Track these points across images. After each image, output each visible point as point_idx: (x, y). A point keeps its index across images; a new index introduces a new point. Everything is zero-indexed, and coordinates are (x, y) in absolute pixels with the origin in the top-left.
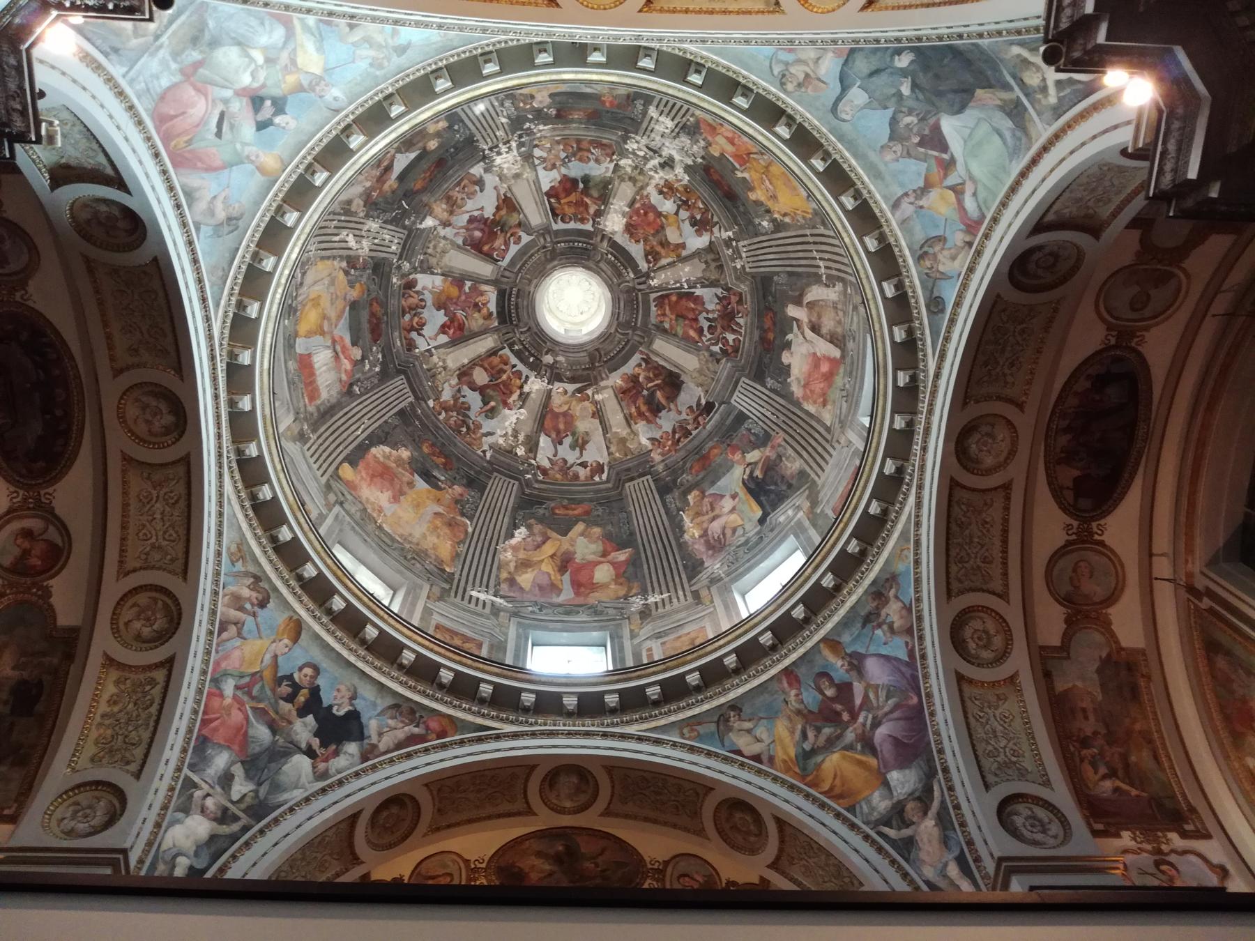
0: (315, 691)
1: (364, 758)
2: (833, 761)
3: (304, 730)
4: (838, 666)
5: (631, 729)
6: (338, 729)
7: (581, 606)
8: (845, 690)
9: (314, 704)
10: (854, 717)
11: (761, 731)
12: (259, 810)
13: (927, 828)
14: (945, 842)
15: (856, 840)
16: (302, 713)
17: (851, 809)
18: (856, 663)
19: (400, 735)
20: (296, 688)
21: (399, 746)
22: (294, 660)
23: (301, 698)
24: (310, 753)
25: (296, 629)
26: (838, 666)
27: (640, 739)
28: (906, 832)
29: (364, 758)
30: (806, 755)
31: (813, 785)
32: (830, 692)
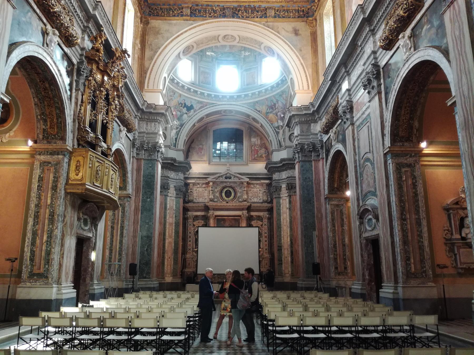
0: (185, 104)
1: (194, 112)
2: (271, 115)
3: (185, 110)
4: (275, 101)
5: (238, 103)
6: (189, 108)
7: (230, 53)
8: (275, 105)
9: (185, 106)
10: (275, 109)
11: (261, 107)
12: (182, 125)
13: (281, 131)
14: (283, 135)
15: (271, 130)
16: (184, 108)
17: (272, 124)
18: (277, 101)
19: (199, 107)
20: (182, 104)
21: (200, 109)
22: (181, 100)
23: (183, 106)
24: (186, 114)
25: (180, 95)
26: (275, 101)
27: (240, 106)
28: (279, 131)
29: (194, 112)
30: (268, 113)
31: (267, 118)
32: (273, 104)
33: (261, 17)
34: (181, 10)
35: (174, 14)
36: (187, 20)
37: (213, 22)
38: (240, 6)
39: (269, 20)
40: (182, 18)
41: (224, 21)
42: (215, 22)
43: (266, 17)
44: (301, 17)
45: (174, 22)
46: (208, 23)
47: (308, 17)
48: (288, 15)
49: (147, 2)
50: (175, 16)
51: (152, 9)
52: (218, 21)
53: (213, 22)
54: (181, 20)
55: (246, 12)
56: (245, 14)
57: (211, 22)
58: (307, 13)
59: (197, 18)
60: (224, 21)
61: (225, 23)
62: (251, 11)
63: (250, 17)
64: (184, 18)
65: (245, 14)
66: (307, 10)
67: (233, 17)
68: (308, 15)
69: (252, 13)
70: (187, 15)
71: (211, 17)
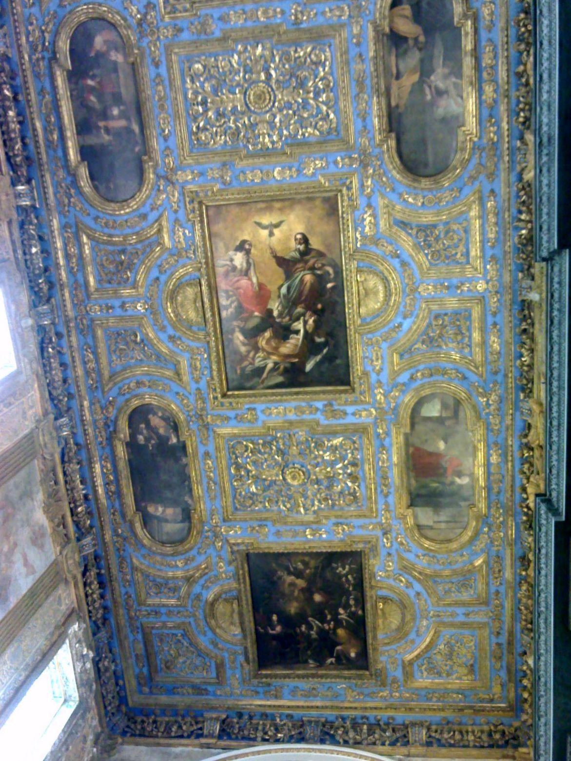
33: (393, 744)
34: (199, 726)
35: (180, 733)
36: (208, 746)
37: (270, 751)
38: (343, 719)
39: (413, 750)
40: (197, 742)
41: (298, 750)
42: (276, 751)
43: (407, 744)
44: (499, 747)
45: (179, 749)
46: (259, 753)
47: (516, 747)
48: (462, 740)
49: (127, 705)
50: (182, 737)
51: (135, 722)
52: (283, 750)
53: (270, 751)
54: (194, 746)
55: (355, 731)
56: (351, 734)
57: (265, 752)
58: (514, 738)
59: (233, 743)
60: (298, 750)
61: (302, 753)
62: (369, 730)
63: (365, 742)
64: (203, 741)
65: (351, 734)
66: (512, 730)
67: (322, 741)
68: (516, 743)
69: (371, 732)
70: (211, 736)
71: (267, 740)
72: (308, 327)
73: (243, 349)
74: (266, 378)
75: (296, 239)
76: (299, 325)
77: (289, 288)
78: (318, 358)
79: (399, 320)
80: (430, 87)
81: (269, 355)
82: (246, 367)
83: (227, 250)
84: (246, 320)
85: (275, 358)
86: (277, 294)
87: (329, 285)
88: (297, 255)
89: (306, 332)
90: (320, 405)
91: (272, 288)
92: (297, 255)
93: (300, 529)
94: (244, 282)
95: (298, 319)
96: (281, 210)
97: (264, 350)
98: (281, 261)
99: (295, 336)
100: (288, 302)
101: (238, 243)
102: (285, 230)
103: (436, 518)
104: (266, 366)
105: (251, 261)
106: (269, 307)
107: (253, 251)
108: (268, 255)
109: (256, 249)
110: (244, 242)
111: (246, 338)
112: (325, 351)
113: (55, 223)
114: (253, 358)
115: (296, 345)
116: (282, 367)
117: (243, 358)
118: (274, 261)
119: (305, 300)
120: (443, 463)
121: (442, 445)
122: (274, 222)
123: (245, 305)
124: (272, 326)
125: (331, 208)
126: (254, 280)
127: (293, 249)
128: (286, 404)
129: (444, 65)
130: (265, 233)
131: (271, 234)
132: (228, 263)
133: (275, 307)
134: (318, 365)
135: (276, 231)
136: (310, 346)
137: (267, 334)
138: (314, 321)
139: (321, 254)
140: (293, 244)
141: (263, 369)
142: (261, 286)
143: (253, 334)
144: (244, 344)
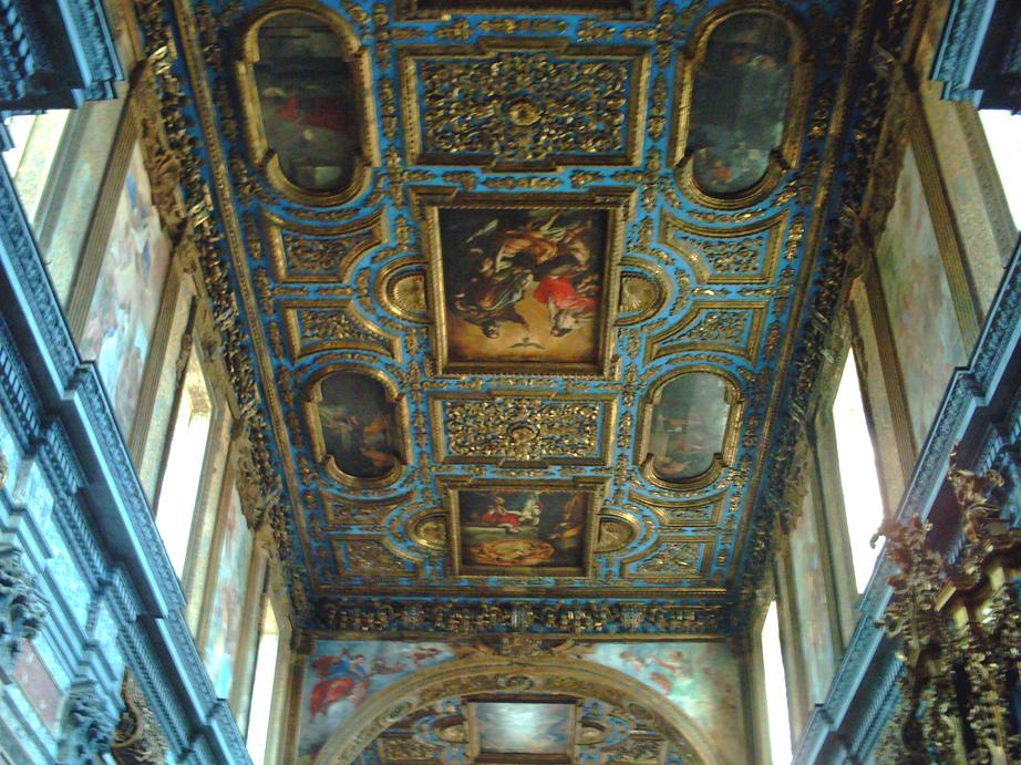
72: (491, 263)
73: (579, 245)
74: (553, 215)
75: (498, 334)
76: (500, 265)
77: (511, 297)
78: (480, 233)
79: (375, 266)
80: (353, 423)
81: (549, 237)
82: (580, 227)
83: (580, 330)
84: (569, 272)
85: (538, 235)
86: (526, 294)
87: (462, 295)
88: (497, 323)
89: (494, 260)
90: (481, 189)
91: (530, 299)
92: (497, 323)
93: (522, 33)
94: (564, 305)
95: (502, 271)
96: (512, 355)
97: (551, 244)
98: (519, 319)
99: (507, 256)
100: (512, 286)
101: (566, 335)
102: (504, 340)
103: (306, 42)
104: (552, 226)
105: (554, 321)
106: (538, 283)
107: (550, 328)
108: (532, 325)
109: (546, 331)
110: (559, 335)
111: (572, 256)
112: (471, 239)
113: (781, 364)
114: (566, 236)
115: (507, 246)
116: (529, 226)
117: (580, 236)
118: (526, 320)
119: (493, 286)
120: (302, 112)
121: (308, 135)
122: (522, 348)
123: (568, 285)
124: (536, 266)
125: (455, 353)
126: (552, 306)
127: (502, 328)
128: (525, 189)
129: (340, 435)
130: (531, 341)
131: (526, 339)
132: (581, 320)
133: (530, 282)
134: (482, 226)
135: (521, 341)
136: (491, 246)
137: (544, 259)
138: (482, 268)
139: (472, 321)
140: (501, 331)
141: (555, 225)
142: (546, 301)
143: (564, 257)
144: (577, 250)
